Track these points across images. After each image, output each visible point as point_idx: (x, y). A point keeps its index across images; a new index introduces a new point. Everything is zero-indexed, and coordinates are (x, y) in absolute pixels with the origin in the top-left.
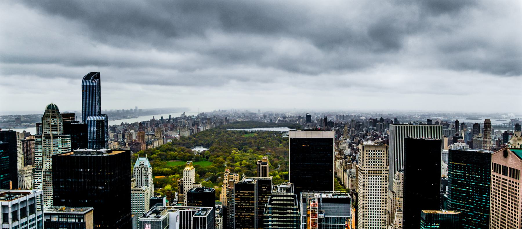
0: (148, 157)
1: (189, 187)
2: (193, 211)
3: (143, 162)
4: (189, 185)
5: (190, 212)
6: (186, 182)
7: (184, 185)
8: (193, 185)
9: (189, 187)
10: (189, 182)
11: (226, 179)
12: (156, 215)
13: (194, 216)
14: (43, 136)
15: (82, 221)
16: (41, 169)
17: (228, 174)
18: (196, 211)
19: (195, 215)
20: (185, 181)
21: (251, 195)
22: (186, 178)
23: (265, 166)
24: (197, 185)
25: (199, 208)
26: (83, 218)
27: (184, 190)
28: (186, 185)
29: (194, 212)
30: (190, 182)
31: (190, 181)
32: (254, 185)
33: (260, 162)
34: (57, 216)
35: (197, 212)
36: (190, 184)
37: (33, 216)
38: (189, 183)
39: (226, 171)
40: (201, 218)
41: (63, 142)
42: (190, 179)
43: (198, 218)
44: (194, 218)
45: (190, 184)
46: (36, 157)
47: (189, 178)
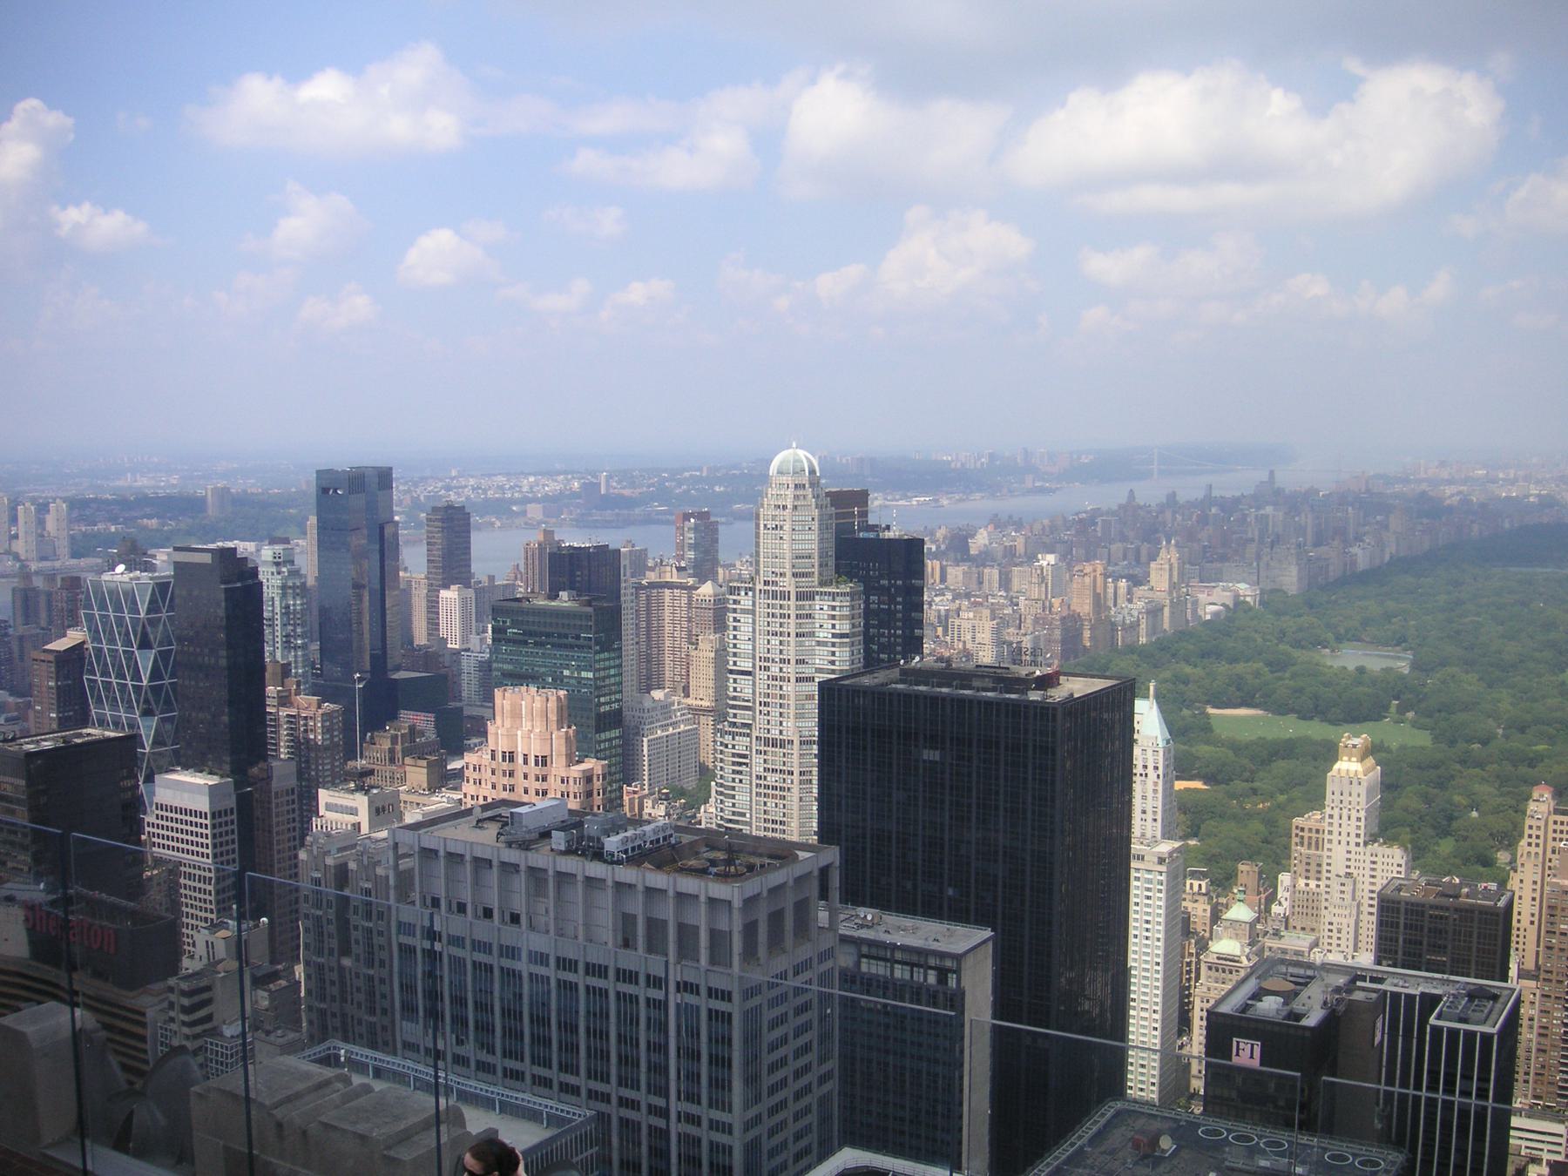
0: (1157, 697)
1: (1352, 856)
2: (1423, 995)
5: (1411, 998)
6: (1335, 829)
7: (1327, 846)
9: (1352, 856)
10: (1353, 832)
11: (1534, 832)
12: (1285, 1003)
13: (1432, 1020)
14: (759, 586)
15: (952, 982)
16: (748, 726)
17: (1543, 808)
18: (1437, 999)
19: (1439, 1017)
20: (1331, 824)
22: (1336, 812)
24: (1388, 851)
25: (1458, 982)
26: (958, 972)
27: (1325, 867)
28: (1334, 845)
29: (1430, 1001)
30: (1358, 836)
34: (851, 949)
35: (1445, 999)
36: (1358, 844)
37: (805, 952)
38: (1353, 840)
39: (1535, 795)
40: (1470, 1036)
41: (833, 617)
43: (1453, 1034)
44: (1437, 1031)
45: (1358, 844)
46: (731, 672)
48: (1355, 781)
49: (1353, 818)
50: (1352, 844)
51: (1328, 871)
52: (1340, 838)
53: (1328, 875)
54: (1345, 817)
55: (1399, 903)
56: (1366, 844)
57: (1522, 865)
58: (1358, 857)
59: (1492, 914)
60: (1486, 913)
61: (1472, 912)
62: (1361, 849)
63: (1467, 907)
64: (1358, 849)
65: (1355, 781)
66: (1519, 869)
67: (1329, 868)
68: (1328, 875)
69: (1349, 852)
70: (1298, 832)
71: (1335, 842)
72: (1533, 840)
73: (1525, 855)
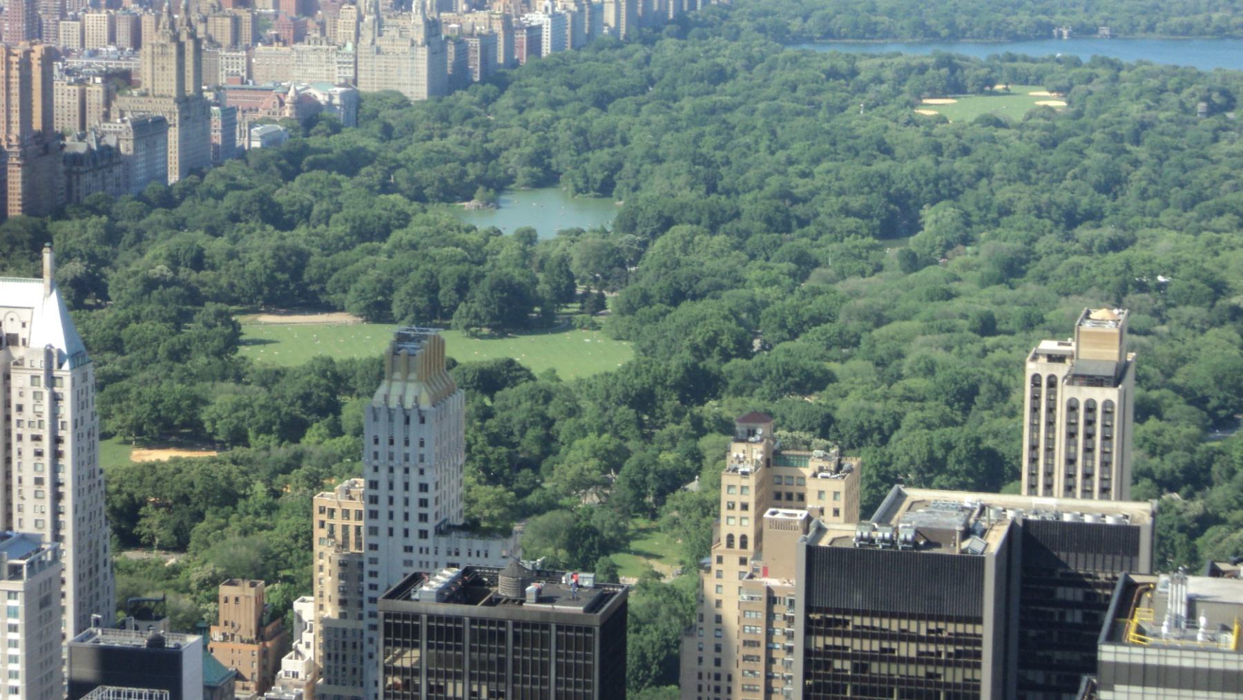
1: (415, 556)
3: (25, 315)
4: (414, 540)
8: (443, 541)
10: (414, 510)
11: (738, 499)
21: (955, 661)
23: (1101, 395)
24: (478, 544)
27: (367, 580)
30: (423, 518)
31: (424, 503)
32: (975, 563)
33: (1054, 358)
36: (423, 534)
38: (415, 525)
42: (424, 488)
45: (423, 534)
47: (415, 479)
48: (414, 419)
49: (414, 487)
50: (414, 534)
51: (373, 587)
52: (391, 524)
53: (373, 594)
54: (399, 485)
55: (416, 617)
56: (440, 531)
57: (720, 560)
58: (423, 557)
59: (579, 629)
60: (569, 629)
61: (546, 626)
62: (429, 543)
63: (537, 618)
64: (424, 543)
65: (414, 419)
66: (715, 567)
67: (373, 581)
68: (373, 594)
69: (408, 549)
70: (324, 517)
71: (383, 532)
72: (737, 511)
73: (724, 541)
